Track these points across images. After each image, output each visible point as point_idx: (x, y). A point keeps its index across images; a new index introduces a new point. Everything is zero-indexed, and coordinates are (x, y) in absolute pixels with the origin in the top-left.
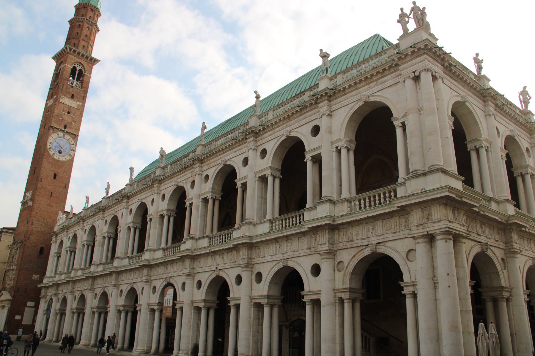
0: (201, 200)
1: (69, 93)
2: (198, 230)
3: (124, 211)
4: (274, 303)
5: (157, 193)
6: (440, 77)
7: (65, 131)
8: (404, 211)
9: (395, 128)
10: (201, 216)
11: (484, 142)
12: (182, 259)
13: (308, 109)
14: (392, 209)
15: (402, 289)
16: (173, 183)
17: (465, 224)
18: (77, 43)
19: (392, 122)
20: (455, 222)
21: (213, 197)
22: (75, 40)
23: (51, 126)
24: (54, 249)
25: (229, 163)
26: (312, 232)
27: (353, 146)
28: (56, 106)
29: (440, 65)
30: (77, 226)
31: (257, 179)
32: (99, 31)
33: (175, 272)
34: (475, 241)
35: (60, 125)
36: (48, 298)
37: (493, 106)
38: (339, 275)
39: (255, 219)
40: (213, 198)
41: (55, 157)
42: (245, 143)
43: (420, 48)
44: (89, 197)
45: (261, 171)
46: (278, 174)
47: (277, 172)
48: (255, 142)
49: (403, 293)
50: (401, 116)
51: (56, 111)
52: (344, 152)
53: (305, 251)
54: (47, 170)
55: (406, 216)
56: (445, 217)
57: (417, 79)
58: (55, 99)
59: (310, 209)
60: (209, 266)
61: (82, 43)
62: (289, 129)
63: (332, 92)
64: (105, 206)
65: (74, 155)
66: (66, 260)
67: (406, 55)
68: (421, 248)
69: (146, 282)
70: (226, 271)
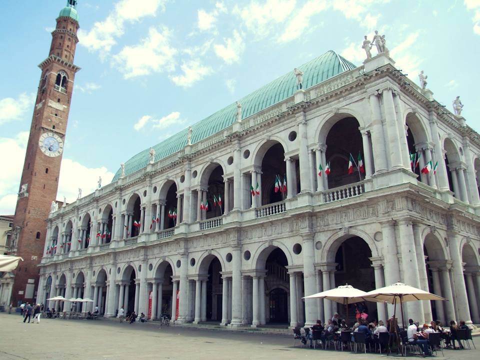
0: (191, 192)
1: (55, 97)
3: (118, 201)
5: (149, 186)
6: (398, 94)
8: (371, 202)
9: (361, 135)
10: (191, 206)
11: (429, 145)
13: (286, 118)
14: (362, 201)
16: (164, 177)
19: (359, 131)
24: (50, 234)
25: (215, 161)
27: (325, 148)
28: (45, 109)
29: (397, 84)
31: (242, 175)
32: (78, 41)
34: (426, 225)
35: (49, 126)
36: (47, 276)
37: (436, 114)
38: (318, 253)
39: (242, 207)
41: (46, 154)
43: (383, 71)
46: (260, 171)
49: (372, 266)
50: (367, 126)
51: (45, 114)
52: (318, 154)
53: (287, 233)
54: (39, 166)
57: (379, 96)
58: (43, 103)
59: (290, 200)
61: (65, 53)
62: (269, 134)
67: (371, 77)
68: (386, 232)
69: (143, 261)
70: (218, 250)
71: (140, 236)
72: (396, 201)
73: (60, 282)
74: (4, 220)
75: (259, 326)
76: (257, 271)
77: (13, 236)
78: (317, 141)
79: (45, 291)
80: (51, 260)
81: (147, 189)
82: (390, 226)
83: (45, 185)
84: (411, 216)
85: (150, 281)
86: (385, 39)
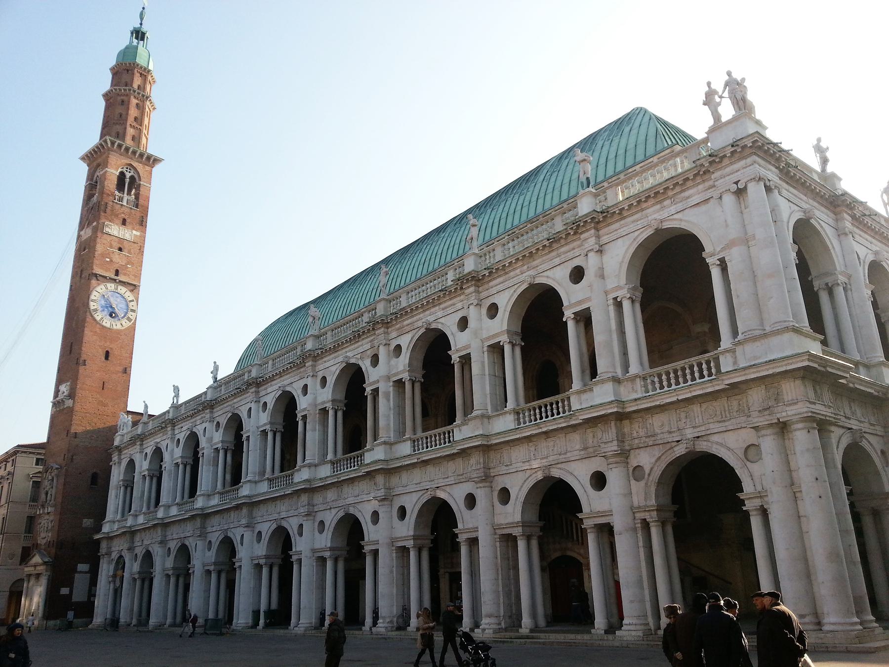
0: (391, 384)
1: (117, 216)
2: (392, 429)
3: (253, 405)
4: (532, 533)
7: (118, 281)
10: (394, 408)
11: (840, 277)
12: (370, 475)
15: (742, 503)
16: (341, 359)
17: (831, 405)
18: (121, 132)
19: (704, 259)
20: (819, 402)
21: (412, 378)
22: (117, 126)
23: (92, 273)
24: (117, 475)
25: (433, 326)
26: (587, 425)
27: (639, 294)
28: (98, 240)
29: (773, 169)
30: (161, 434)
31: (485, 349)
33: (356, 497)
35: (107, 270)
36: (115, 555)
37: (850, 218)
38: (637, 487)
39: (489, 408)
40: (412, 380)
41: (104, 324)
42: (460, 295)
43: (746, 146)
44: (179, 387)
45: (494, 336)
46: (518, 340)
47: (516, 337)
48: (477, 294)
49: (744, 508)
50: (718, 249)
51: (99, 248)
52: (626, 305)
54: (91, 346)
55: (739, 397)
56: (804, 396)
57: (740, 192)
59: (579, 392)
60: (416, 484)
61: (130, 132)
63: (601, 216)
64: (215, 400)
65: (136, 318)
66: (143, 492)
68: (768, 443)
70: (448, 489)
71: (299, 470)
72: (783, 386)
73: (141, 567)
74: (25, 452)
75: (535, 629)
76: (524, 524)
77: (46, 483)
78: (623, 281)
79: (112, 585)
80: (124, 524)
81: (309, 381)
82: (776, 434)
83: (104, 382)
84: (812, 412)
85: (320, 554)
86: (745, 84)
